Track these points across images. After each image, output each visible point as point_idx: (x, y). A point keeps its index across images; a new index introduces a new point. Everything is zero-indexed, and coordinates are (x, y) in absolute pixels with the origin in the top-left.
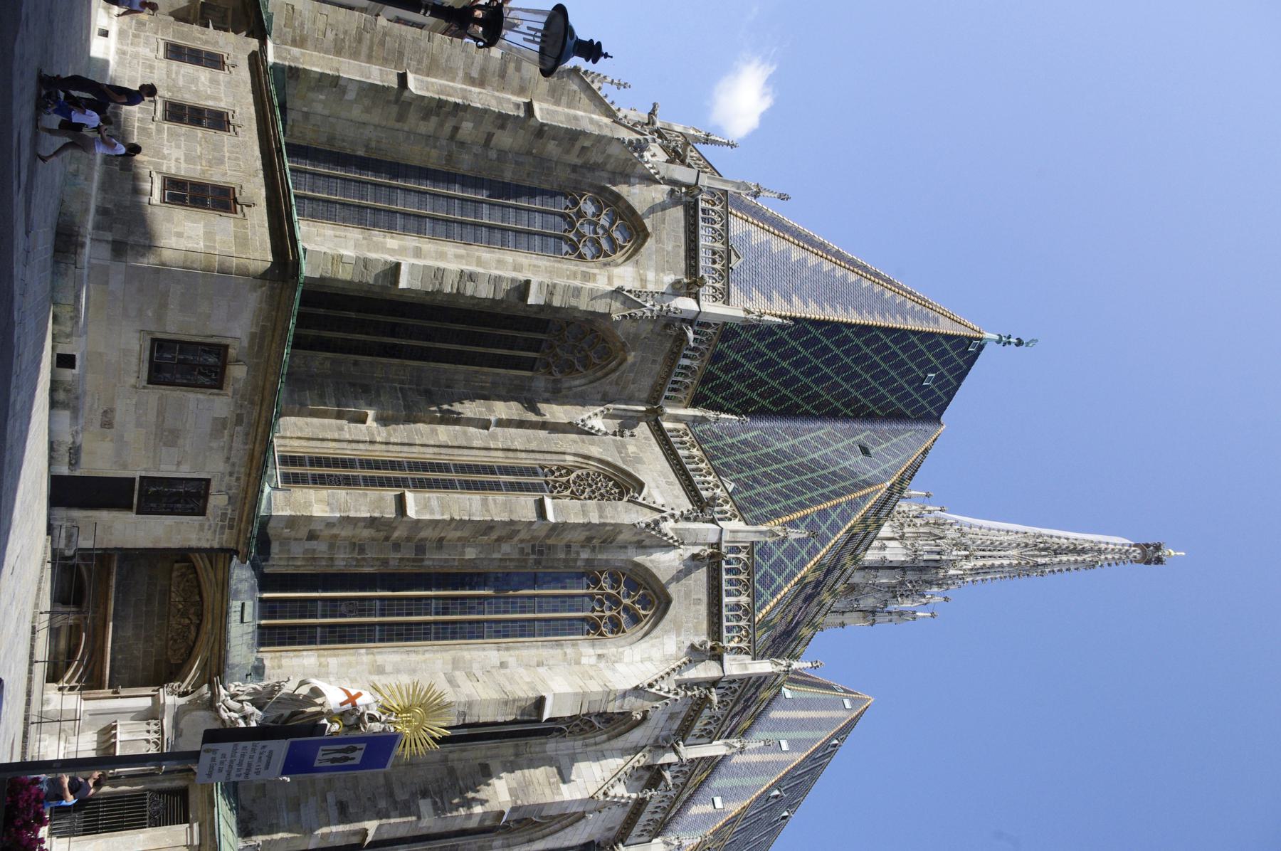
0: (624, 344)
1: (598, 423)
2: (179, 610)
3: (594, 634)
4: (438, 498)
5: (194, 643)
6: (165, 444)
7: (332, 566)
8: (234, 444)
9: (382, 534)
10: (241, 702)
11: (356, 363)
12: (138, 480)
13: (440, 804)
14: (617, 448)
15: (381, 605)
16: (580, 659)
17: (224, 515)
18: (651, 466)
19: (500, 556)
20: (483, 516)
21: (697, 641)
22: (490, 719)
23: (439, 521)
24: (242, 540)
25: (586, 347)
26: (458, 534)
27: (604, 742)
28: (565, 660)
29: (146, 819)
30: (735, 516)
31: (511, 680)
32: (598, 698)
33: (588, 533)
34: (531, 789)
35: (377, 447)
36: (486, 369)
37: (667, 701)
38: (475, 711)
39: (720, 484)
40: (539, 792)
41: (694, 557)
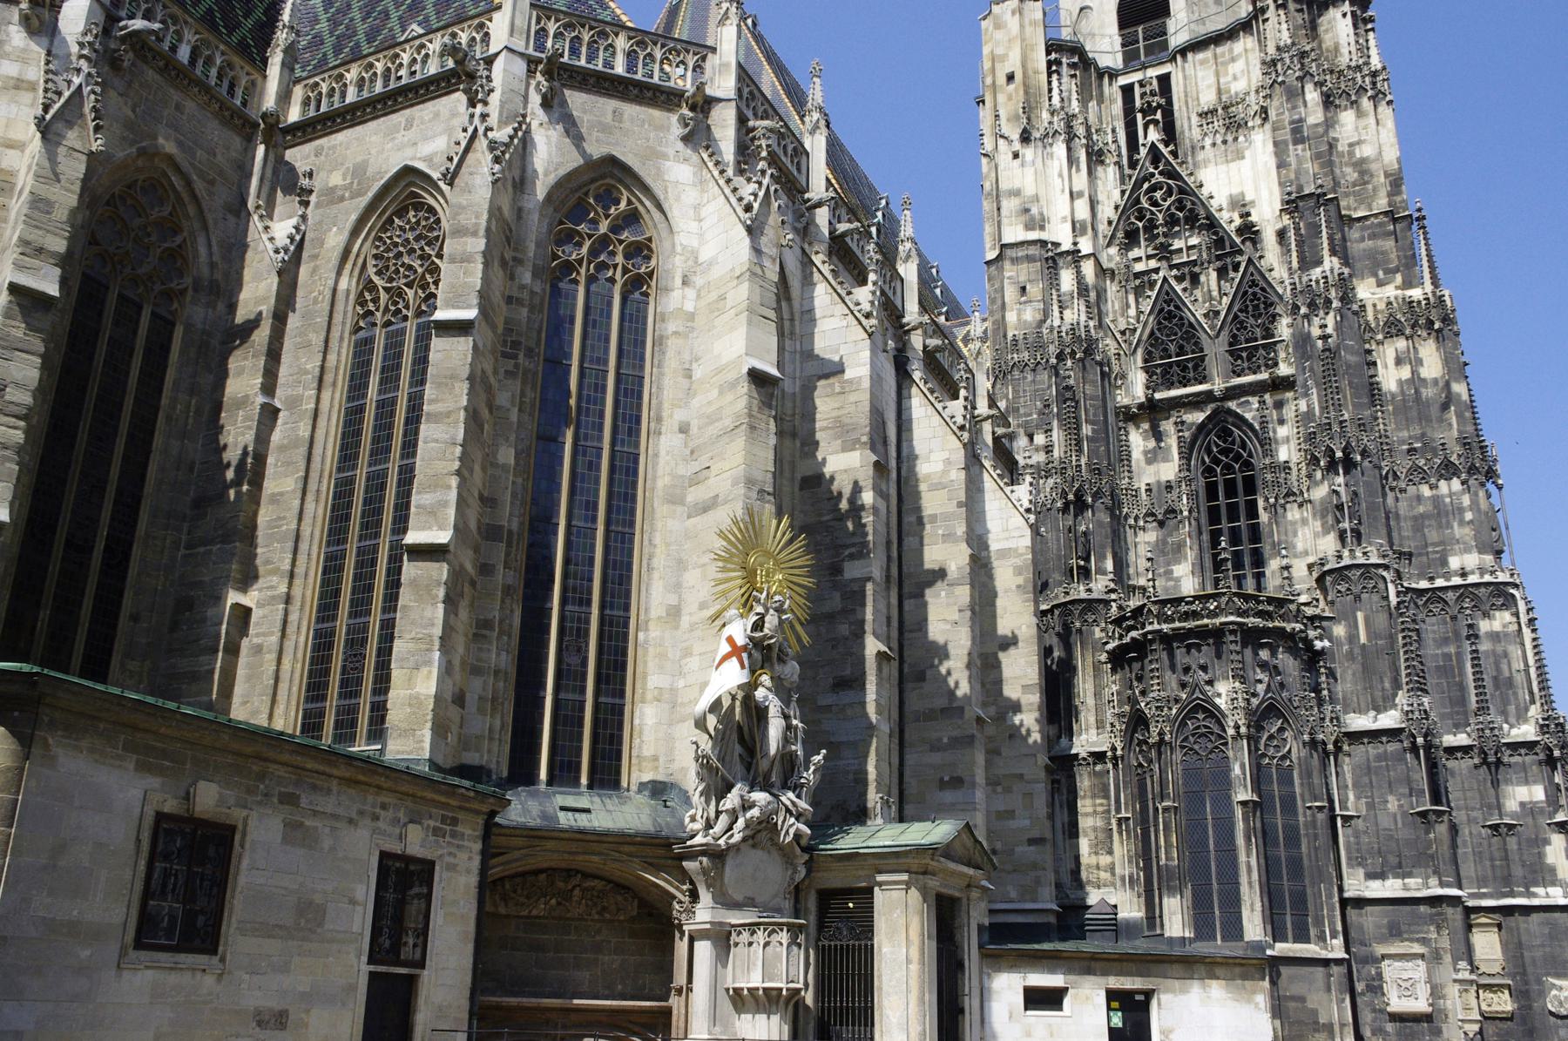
0: (142, 152)
1: (282, 229)
2: (559, 904)
3: (649, 286)
4: (419, 493)
5: (610, 882)
6: (321, 925)
7: (506, 673)
8: (329, 810)
9: (467, 588)
10: (718, 813)
11: (135, 618)
12: (372, 968)
13: (853, 550)
14: (332, 202)
15: (574, 604)
16: (687, 313)
17: (436, 832)
18: (373, 151)
19: (516, 409)
20: (457, 422)
21: (677, 130)
22: (771, 456)
23: (459, 495)
24: (476, 806)
25: (137, 222)
26: (477, 468)
27: (791, 307)
28: (687, 337)
29: (860, 946)
30: (481, 26)
31: (712, 419)
32: (758, 290)
33: (496, 264)
34: (848, 421)
35: (297, 591)
36: (164, 401)
37: (772, 189)
38: (759, 476)
39: (417, 42)
40: (852, 409)
41: (546, 104)
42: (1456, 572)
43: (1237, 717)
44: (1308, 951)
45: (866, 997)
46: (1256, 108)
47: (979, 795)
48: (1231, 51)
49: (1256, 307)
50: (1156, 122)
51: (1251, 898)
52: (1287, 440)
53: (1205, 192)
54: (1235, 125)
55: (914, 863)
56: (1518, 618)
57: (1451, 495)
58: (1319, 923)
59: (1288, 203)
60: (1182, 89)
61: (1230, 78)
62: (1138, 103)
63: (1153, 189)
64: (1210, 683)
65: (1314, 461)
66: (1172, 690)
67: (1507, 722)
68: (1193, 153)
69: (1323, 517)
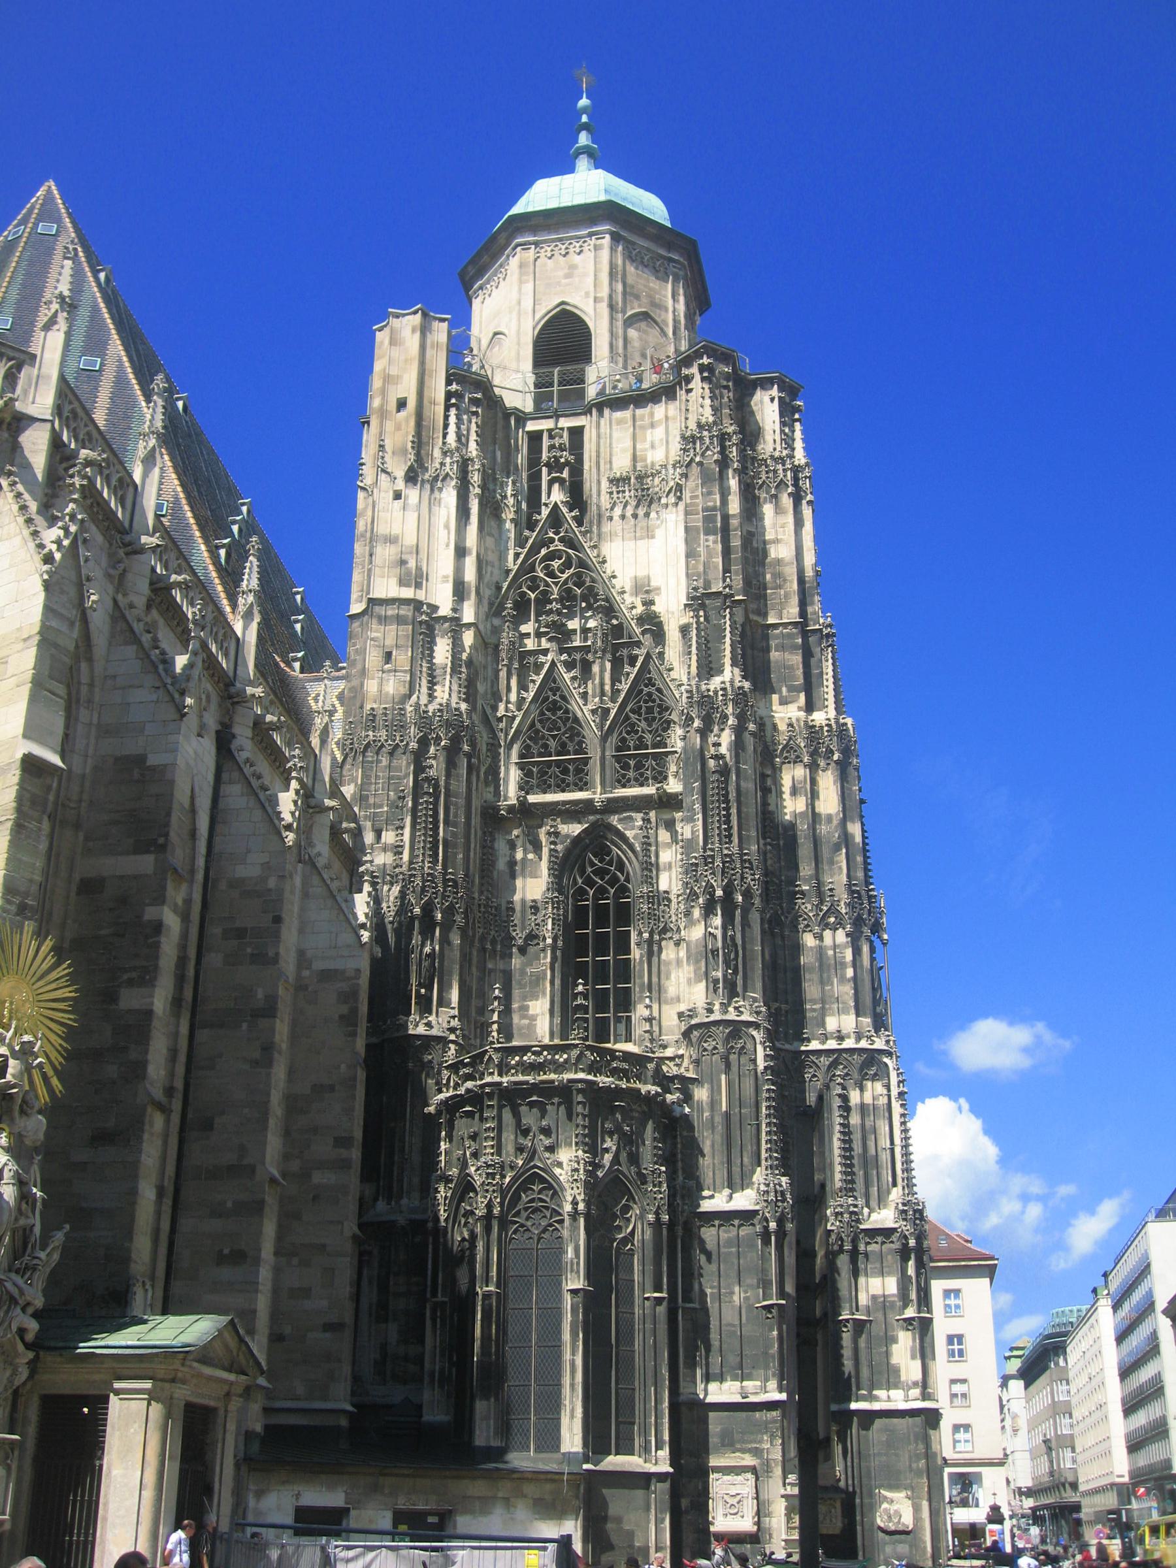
13: (134, 975)
42: (832, 1033)
43: (576, 1191)
44: (630, 1464)
45: (87, 1530)
46: (672, 483)
47: (265, 1274)
48: (652, 415)
49: (650, 710)
50: (561, 481)
51: (571, 1402)
52: (669, 866)
53: (609, 568)
54: (647, 499)
55: (161, 1370)
56: (889, 1090)
57: (835, 947)
58: (645, 1433)
59: (693, 598)
60: (594, 448)
61: (647, 445)
62: (545, 456)
63: (551, 556)
64: (551, 1149)
65: (692, 896)
66: (508, 1155)
67: (868, 1206)
68: (599, 523)
69: (697, 962)
